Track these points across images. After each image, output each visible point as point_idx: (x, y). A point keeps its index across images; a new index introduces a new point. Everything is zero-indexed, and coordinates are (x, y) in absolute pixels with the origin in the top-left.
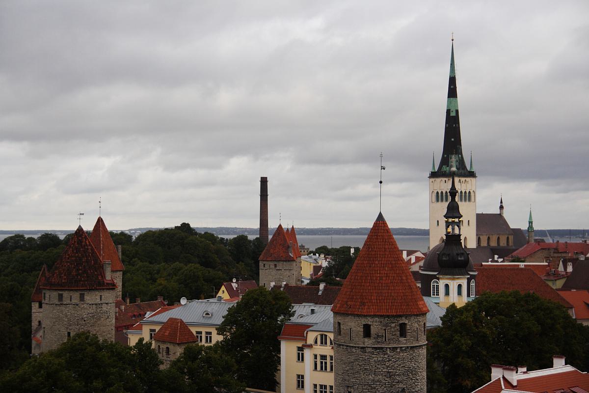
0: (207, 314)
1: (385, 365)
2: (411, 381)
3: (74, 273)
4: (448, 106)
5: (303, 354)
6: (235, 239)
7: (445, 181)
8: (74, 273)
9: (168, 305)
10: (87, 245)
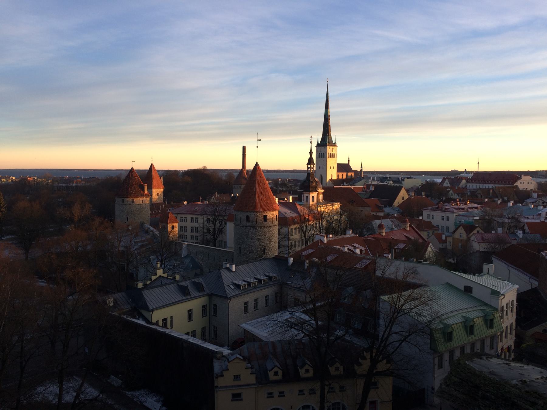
0: (196, 209)
6: (227, 174)
10: (135, 176)
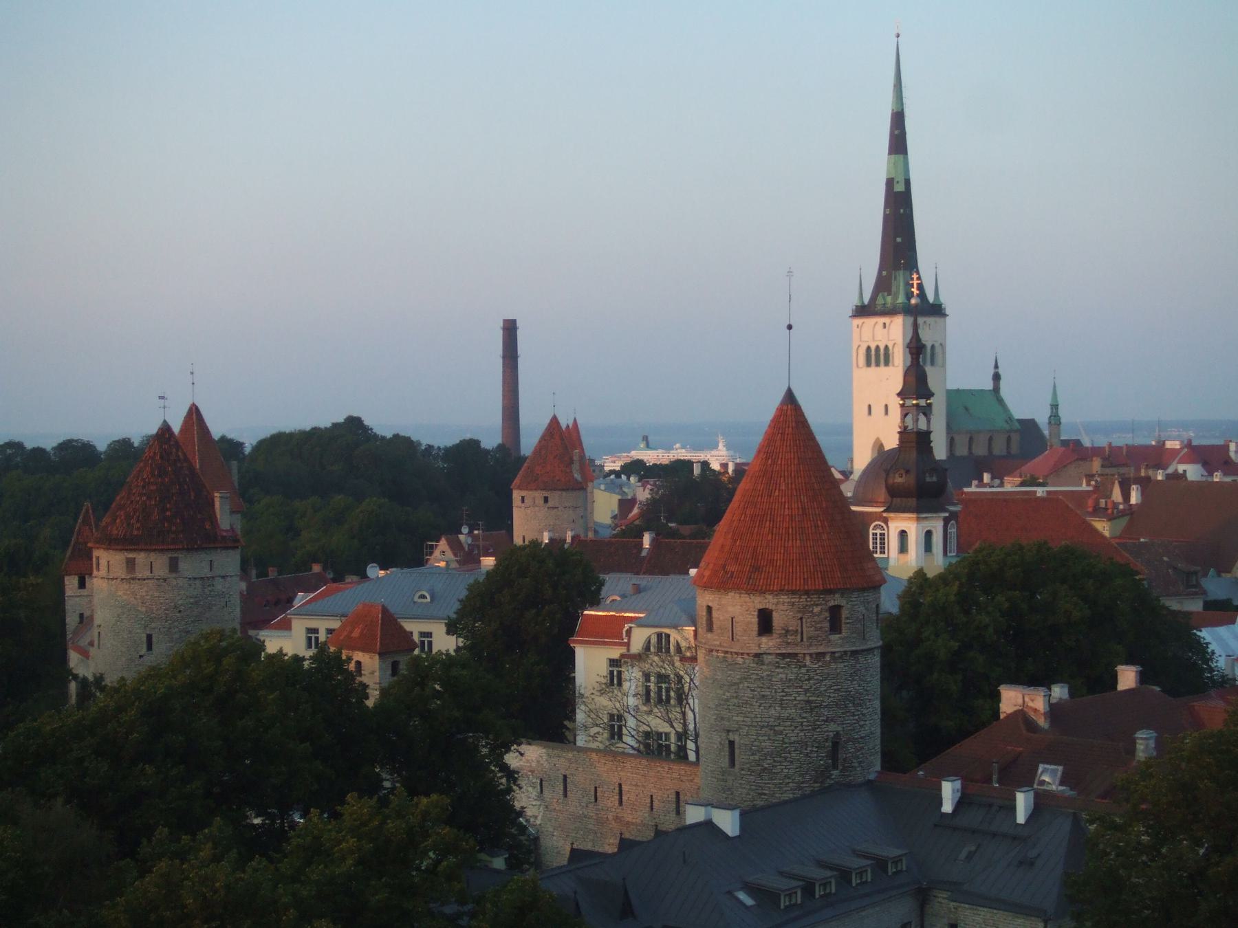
0: (423, 597)
1: (801, 687)
2: (852, 718)
3: (155, 516)
4: (888, 170)
5: (620, 673)
7: (885, 324)
8: (155, 516)
9: (334, 580)
